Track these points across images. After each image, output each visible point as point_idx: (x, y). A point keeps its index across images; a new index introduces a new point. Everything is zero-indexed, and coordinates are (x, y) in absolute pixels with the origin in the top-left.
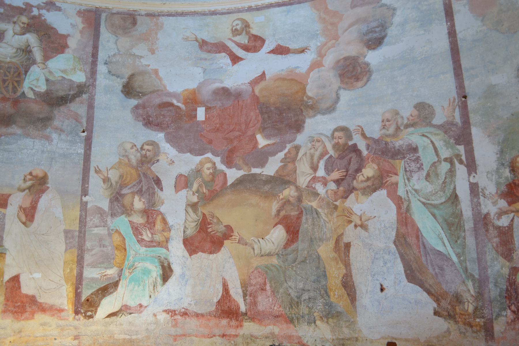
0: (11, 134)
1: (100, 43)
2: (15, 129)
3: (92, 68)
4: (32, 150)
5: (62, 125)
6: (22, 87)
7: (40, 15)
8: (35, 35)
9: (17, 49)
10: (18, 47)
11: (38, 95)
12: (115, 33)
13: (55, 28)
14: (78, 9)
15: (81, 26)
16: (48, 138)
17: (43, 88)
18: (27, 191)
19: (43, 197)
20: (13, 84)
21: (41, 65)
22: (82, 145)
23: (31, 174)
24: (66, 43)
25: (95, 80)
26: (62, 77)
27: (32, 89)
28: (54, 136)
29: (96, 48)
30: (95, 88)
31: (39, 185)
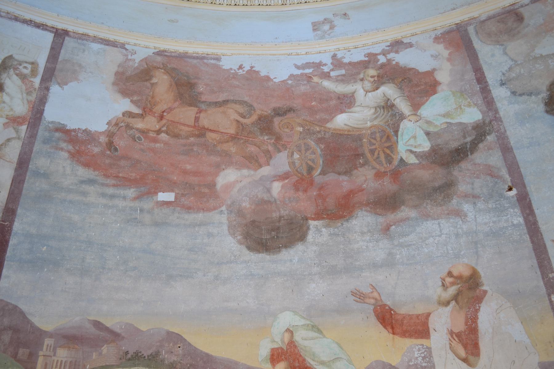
0: (403, 220)
1: (481, 62)
2: (405, 212)
3: (485, 98)
4: (440, 236)
5: (473, 189)
6: (398, 153)
7: (389, 61)
8: (392, 85)
9: (376, 108)
10: (376, 105)
11: (421, 157)
12: (498, 42)
13: (413, 69)
14: (434, 36)
15: (446, 53)
16: (458, 214)
17: (425, 145)
18: (453, 303)
19: (481, 309)
20: (384, 152)
21: (413, 118)
22: (516, 210)
23: (450, 274)
24: (435, 80)
25: (496, 111)
26: (447, 123)
27: (411, 151)
28: (467, 207)
29: (478, 71)
30: (502, 122)
31: (468, 290)
